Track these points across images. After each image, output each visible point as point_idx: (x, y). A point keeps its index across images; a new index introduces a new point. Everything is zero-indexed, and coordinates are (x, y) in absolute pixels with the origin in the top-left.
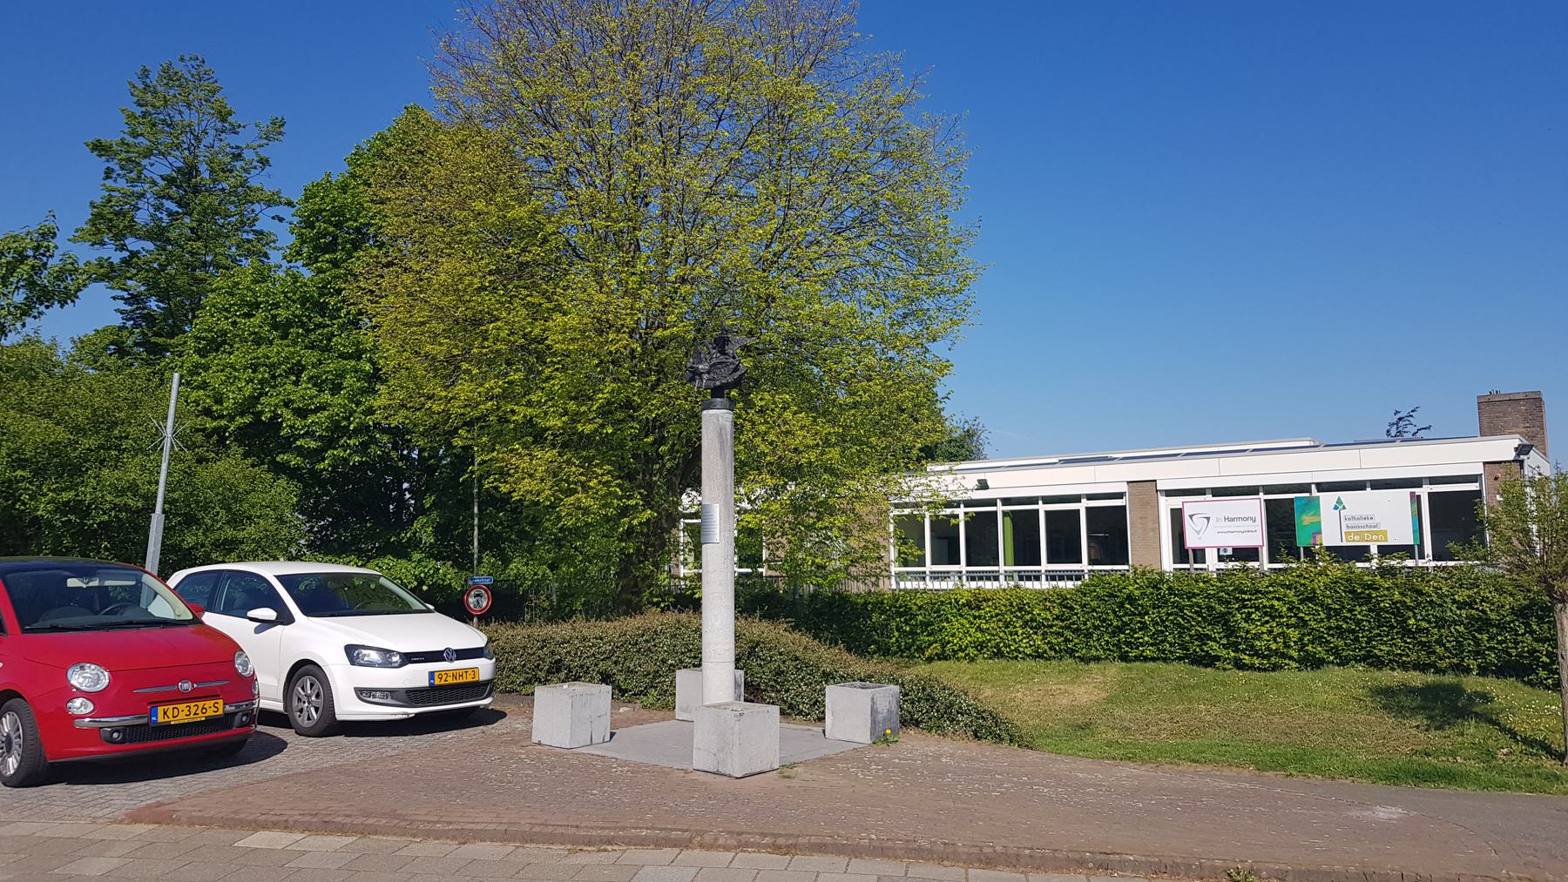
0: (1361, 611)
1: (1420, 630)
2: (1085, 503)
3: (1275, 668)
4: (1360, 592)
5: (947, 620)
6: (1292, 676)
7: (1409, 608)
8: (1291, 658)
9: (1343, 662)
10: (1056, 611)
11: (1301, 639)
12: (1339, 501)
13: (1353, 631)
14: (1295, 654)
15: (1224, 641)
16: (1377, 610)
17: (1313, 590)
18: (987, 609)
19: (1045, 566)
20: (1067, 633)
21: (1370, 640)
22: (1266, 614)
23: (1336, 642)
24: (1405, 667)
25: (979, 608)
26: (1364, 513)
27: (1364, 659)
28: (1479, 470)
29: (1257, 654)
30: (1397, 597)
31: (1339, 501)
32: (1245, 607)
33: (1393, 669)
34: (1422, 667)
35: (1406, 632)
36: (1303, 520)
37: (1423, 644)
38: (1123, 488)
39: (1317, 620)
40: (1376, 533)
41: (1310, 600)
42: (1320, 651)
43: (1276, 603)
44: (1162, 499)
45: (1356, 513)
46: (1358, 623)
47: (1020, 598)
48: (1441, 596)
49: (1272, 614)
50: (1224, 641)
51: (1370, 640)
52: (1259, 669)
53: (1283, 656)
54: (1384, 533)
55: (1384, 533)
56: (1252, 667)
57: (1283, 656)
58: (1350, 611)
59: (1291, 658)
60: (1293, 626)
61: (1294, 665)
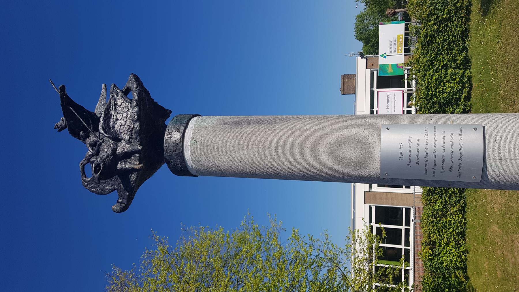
0: (438, 40)
1: (449, 13)
2: (373, 224)
3: (469, 78)
4: (427, 44)
5: (442, 263)
6: (474, 70)
7: (438, 17)
8: (464, 73)
9: (466, 49)
10: (437, 197)
11: (454, 68)
12: (382, 56)
13: (449, 43)
14: (461, 71)
15: (455, 106)
16: (438, 32)
17: (428, 61)
18: (435, 237)
19: (403, 246)
20: (450, 192)
21: (453, 36)
22: (440, 84)
23: (455, 51)
24: (468, 20)
25: (434, 243)
26: (389, 45)
27: (463, 40)
28: (369, 71)
29: (461, 90)
30: (431, 23)
31: (382, 56)
32: (435, 95)
33: (469, 26)
34: (469, 12)
35: (449, 19)
36: (390, 72)
37: (456, 12)
38: (367, 206)
39: (443, 59)
40: (398, 39)
41: (432, 64)
42: (460, 58)
43: (434, 78)
44: (373, 190)
45: (389, 48)
46: (445, 40)
47: (429, 217)
48: (431, 5)
49: (440, 81)
50: (455, 106)
51: (453, 36)
52: (471, 88)
53: (463, 76)
54: (398, 36)
55: (398, 36)
56: (469, 92)
57: (463, 76)
58: (439, 44)
59: (464, 73)
60: (446, 71)
61: (468, 71)
